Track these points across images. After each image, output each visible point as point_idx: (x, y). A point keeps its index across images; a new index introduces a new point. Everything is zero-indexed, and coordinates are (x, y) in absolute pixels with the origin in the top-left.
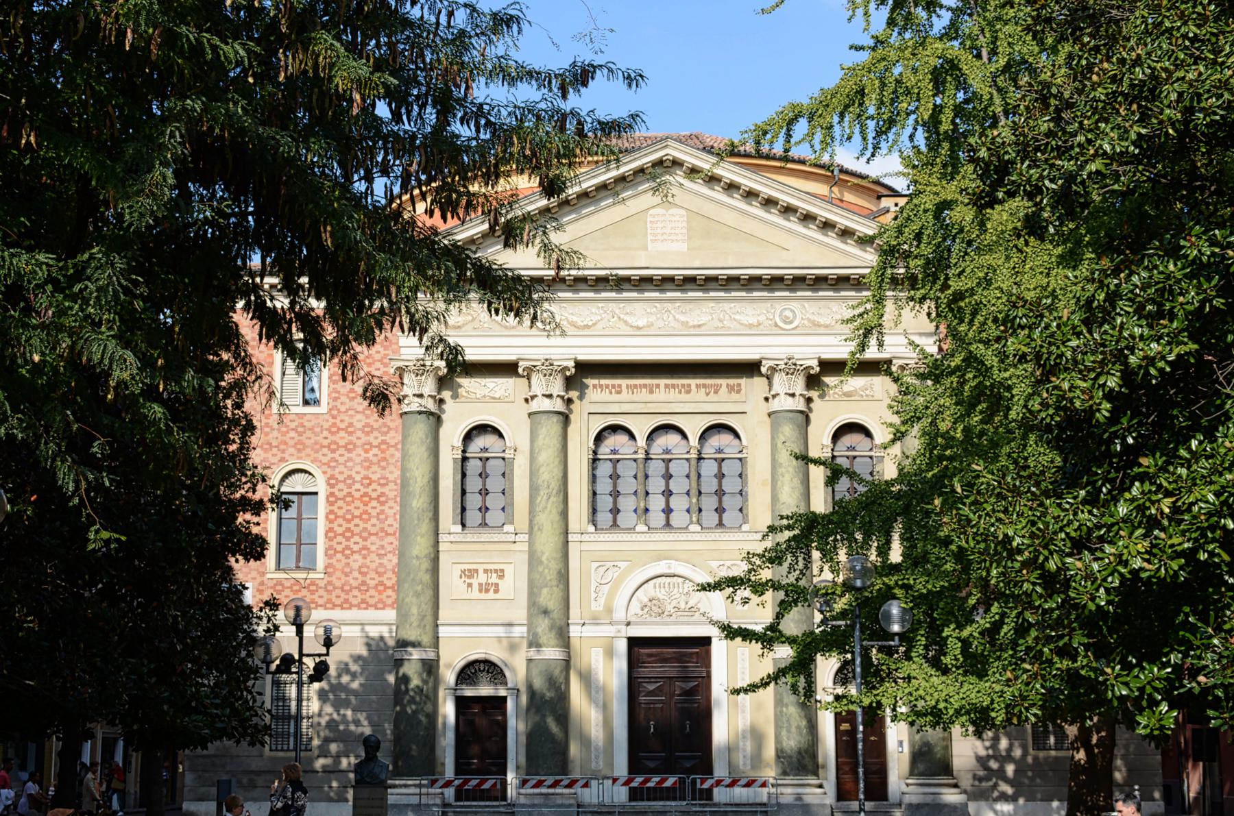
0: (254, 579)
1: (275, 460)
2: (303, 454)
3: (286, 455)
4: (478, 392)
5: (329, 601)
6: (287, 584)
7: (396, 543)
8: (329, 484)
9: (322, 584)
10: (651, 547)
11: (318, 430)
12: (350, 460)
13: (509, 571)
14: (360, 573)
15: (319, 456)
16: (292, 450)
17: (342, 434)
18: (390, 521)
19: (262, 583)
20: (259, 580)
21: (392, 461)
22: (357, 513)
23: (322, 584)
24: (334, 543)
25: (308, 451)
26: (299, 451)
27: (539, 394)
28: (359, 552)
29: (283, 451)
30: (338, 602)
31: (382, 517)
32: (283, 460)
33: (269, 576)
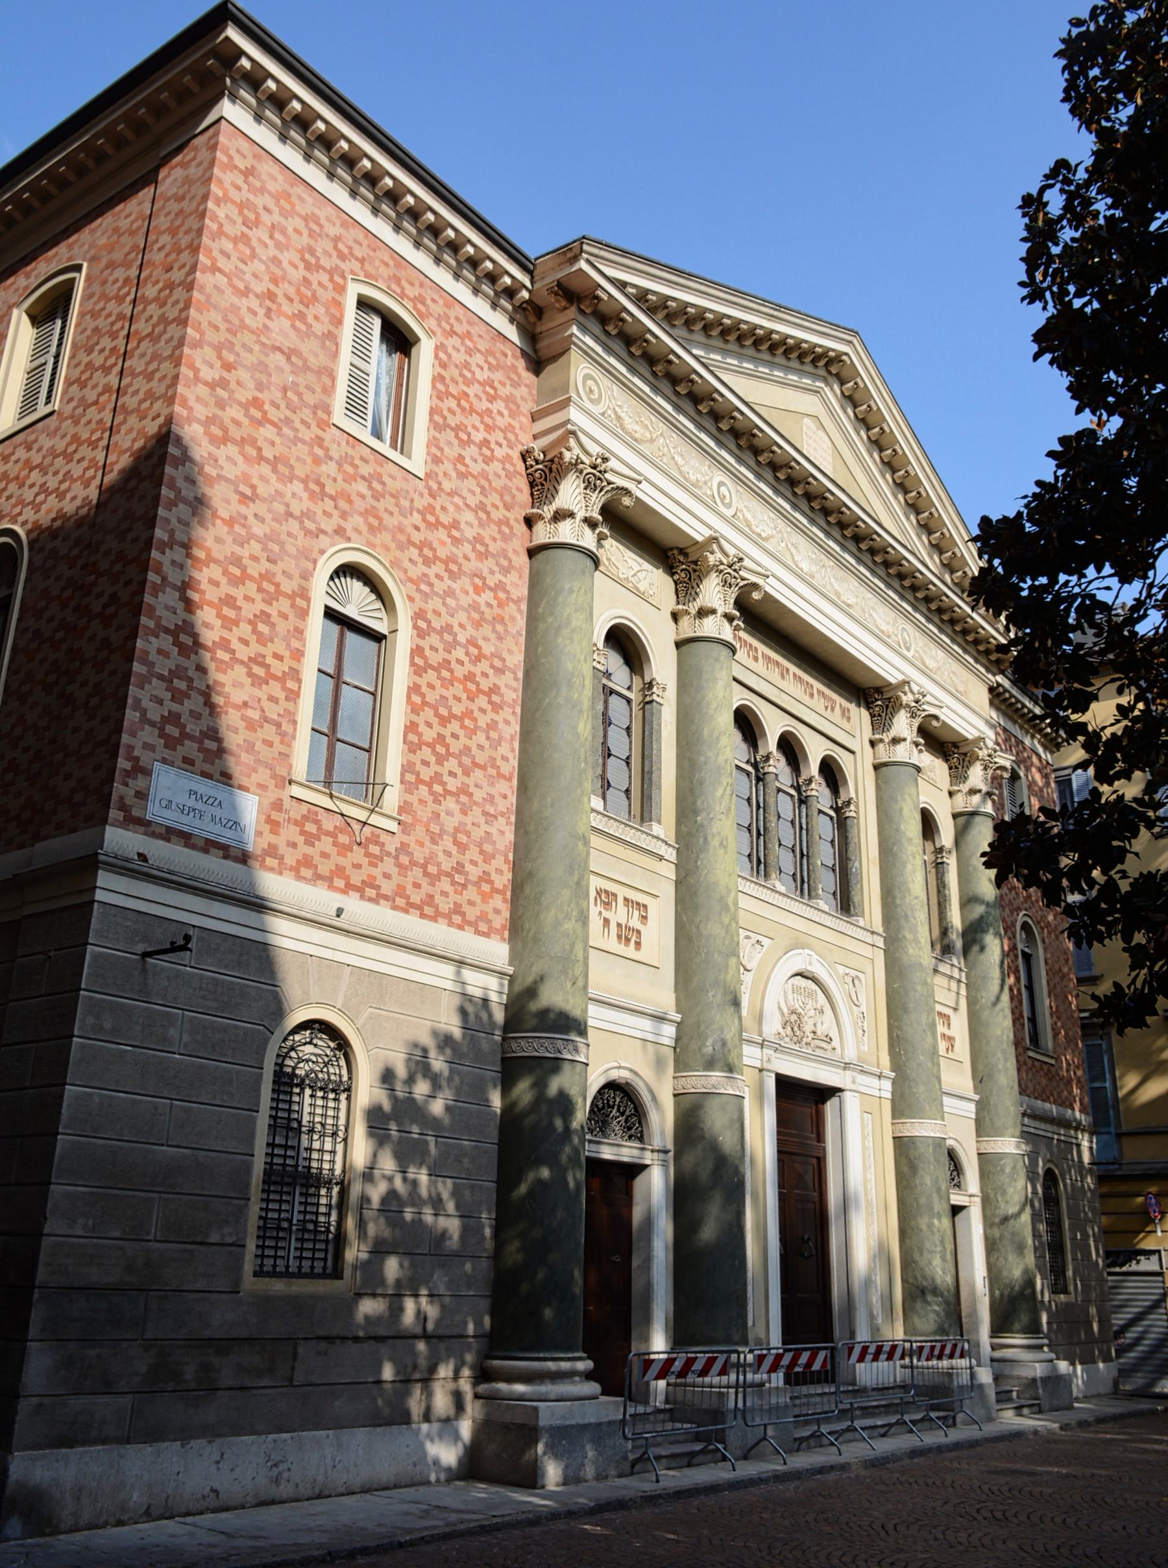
0: (262, 787)
1: (328, 525)
2: (377, 540)
3: (348, 526)
4: (622, 570)
5: (401, 891)
6: (329, 823)
7: (513, 799)
8: (415, 627)
9: (391, 845)
10: (800, 924)
11: (405, 503)
12: (450, 593)
13: (652, 913)
14: (456, 843)
15: (404, 556)
16: (357, 520)
17: (442, 534)
18: (504, 749)
19: (278, 805)
20: (273, 794)
21: (513, 630)
22: (457, 709)
23: (391, 845)
24: (416, 759)
25: (386, 537)
26: (371, 528)
27: (720, 611)
28: (455, 795)
29: (344, 515)
30: (416, 898)
31: (494, 735)
32: (340, 532)
33: (297, 791)
